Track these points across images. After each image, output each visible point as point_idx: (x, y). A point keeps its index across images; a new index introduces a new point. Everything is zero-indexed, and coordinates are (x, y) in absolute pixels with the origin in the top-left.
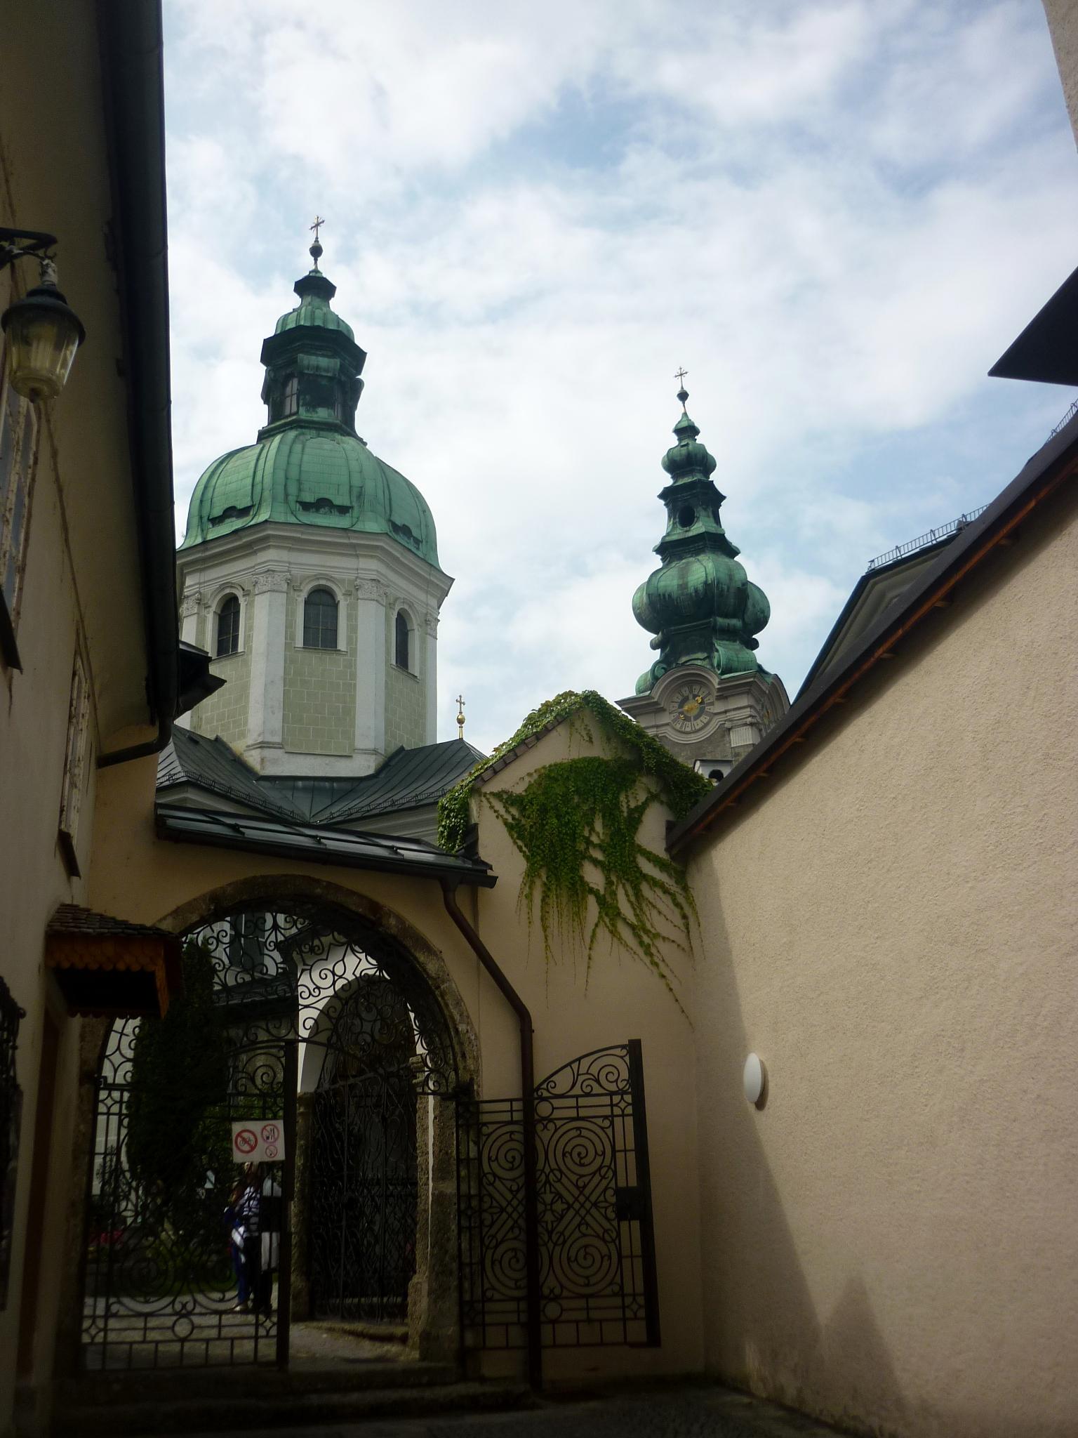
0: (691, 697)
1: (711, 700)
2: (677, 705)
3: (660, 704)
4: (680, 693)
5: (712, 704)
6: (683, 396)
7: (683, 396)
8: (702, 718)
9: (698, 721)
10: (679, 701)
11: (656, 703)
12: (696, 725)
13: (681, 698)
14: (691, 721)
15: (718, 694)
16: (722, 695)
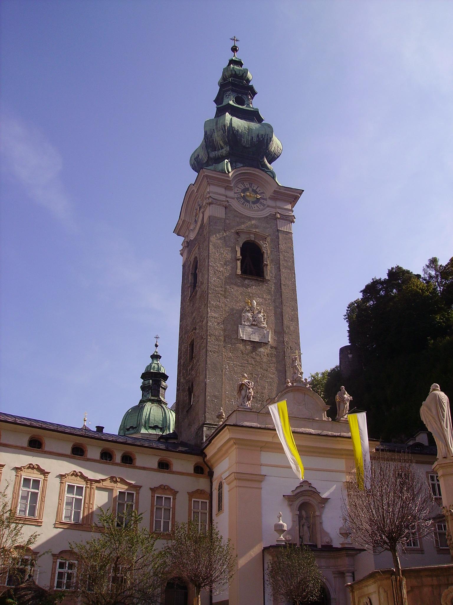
0: (250, 189)
1: (265, 197)
2: (240, 190)
3: (231, 185)
4: (243, 184)
5: (266, 199)
6: (234, 49)
7: (234, 49)
8: (257, 205)
9: (255, 205)
10: (243, 188)
11: (229, 182)
12: (253, 208)
13: (243, 187)
14: (250, 203)
15: (272, 195)
16: (275, 196)
